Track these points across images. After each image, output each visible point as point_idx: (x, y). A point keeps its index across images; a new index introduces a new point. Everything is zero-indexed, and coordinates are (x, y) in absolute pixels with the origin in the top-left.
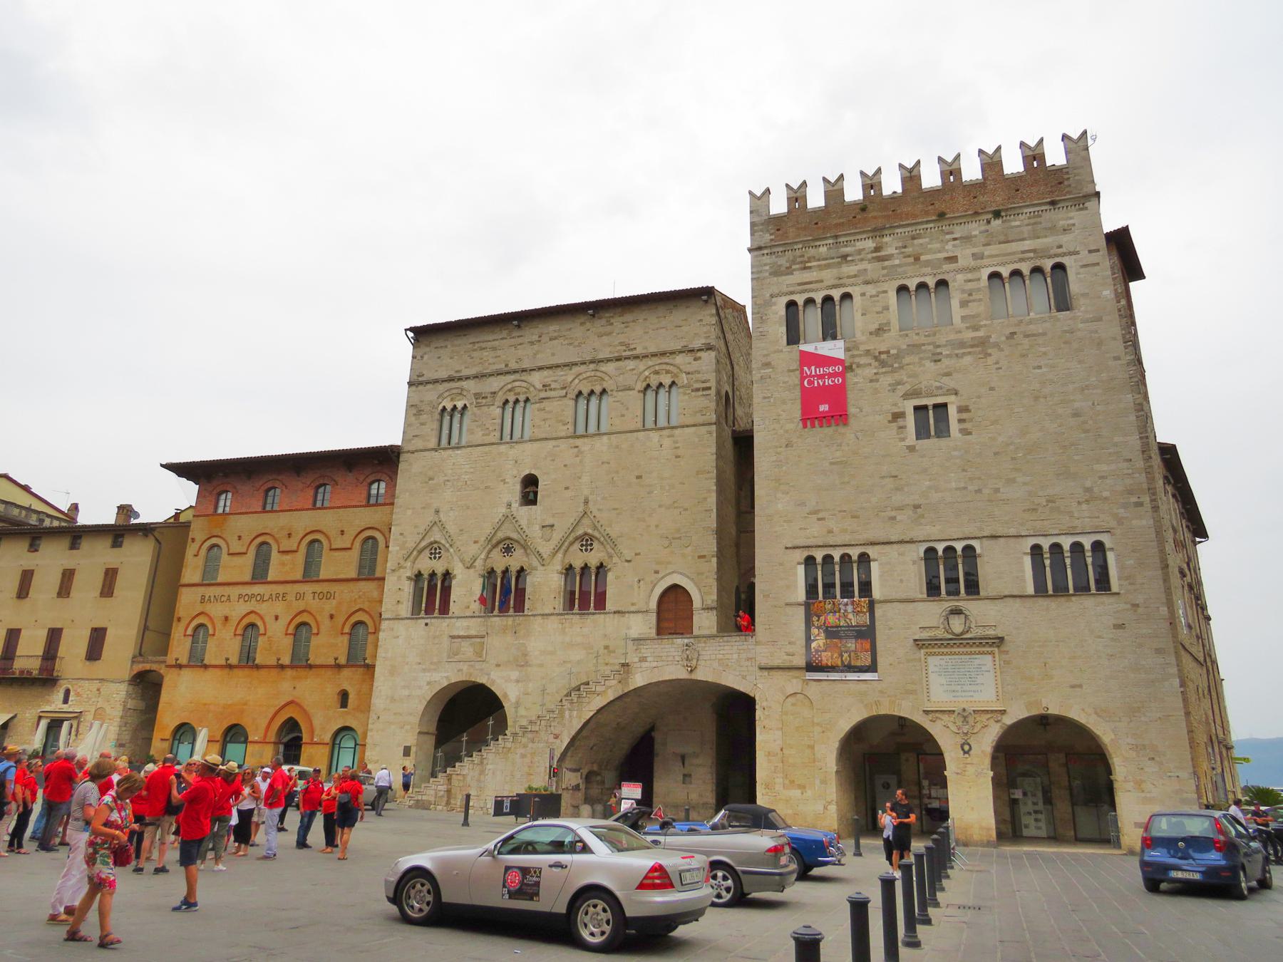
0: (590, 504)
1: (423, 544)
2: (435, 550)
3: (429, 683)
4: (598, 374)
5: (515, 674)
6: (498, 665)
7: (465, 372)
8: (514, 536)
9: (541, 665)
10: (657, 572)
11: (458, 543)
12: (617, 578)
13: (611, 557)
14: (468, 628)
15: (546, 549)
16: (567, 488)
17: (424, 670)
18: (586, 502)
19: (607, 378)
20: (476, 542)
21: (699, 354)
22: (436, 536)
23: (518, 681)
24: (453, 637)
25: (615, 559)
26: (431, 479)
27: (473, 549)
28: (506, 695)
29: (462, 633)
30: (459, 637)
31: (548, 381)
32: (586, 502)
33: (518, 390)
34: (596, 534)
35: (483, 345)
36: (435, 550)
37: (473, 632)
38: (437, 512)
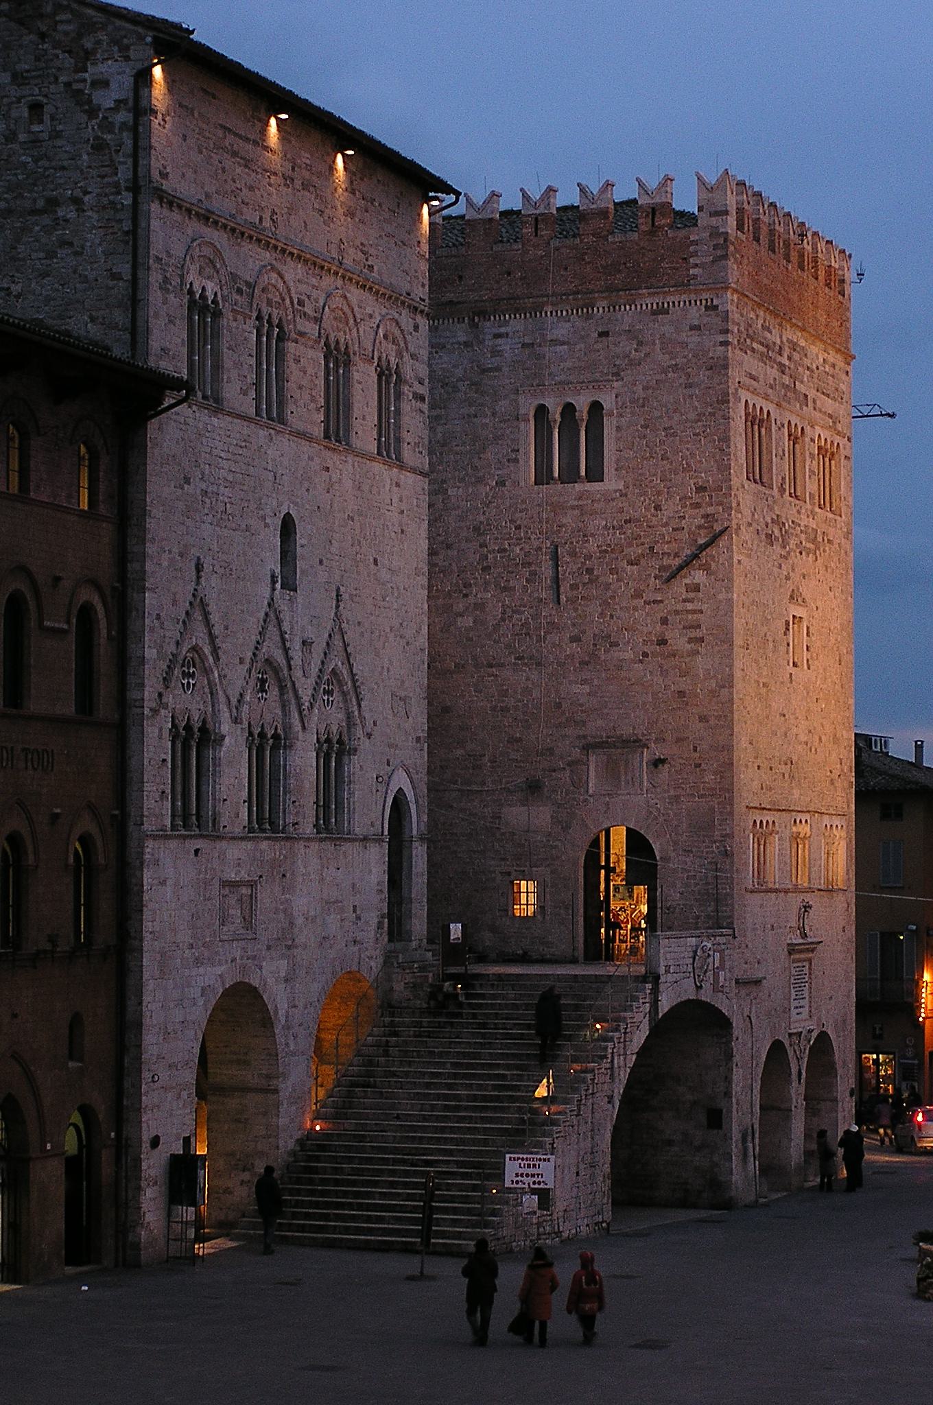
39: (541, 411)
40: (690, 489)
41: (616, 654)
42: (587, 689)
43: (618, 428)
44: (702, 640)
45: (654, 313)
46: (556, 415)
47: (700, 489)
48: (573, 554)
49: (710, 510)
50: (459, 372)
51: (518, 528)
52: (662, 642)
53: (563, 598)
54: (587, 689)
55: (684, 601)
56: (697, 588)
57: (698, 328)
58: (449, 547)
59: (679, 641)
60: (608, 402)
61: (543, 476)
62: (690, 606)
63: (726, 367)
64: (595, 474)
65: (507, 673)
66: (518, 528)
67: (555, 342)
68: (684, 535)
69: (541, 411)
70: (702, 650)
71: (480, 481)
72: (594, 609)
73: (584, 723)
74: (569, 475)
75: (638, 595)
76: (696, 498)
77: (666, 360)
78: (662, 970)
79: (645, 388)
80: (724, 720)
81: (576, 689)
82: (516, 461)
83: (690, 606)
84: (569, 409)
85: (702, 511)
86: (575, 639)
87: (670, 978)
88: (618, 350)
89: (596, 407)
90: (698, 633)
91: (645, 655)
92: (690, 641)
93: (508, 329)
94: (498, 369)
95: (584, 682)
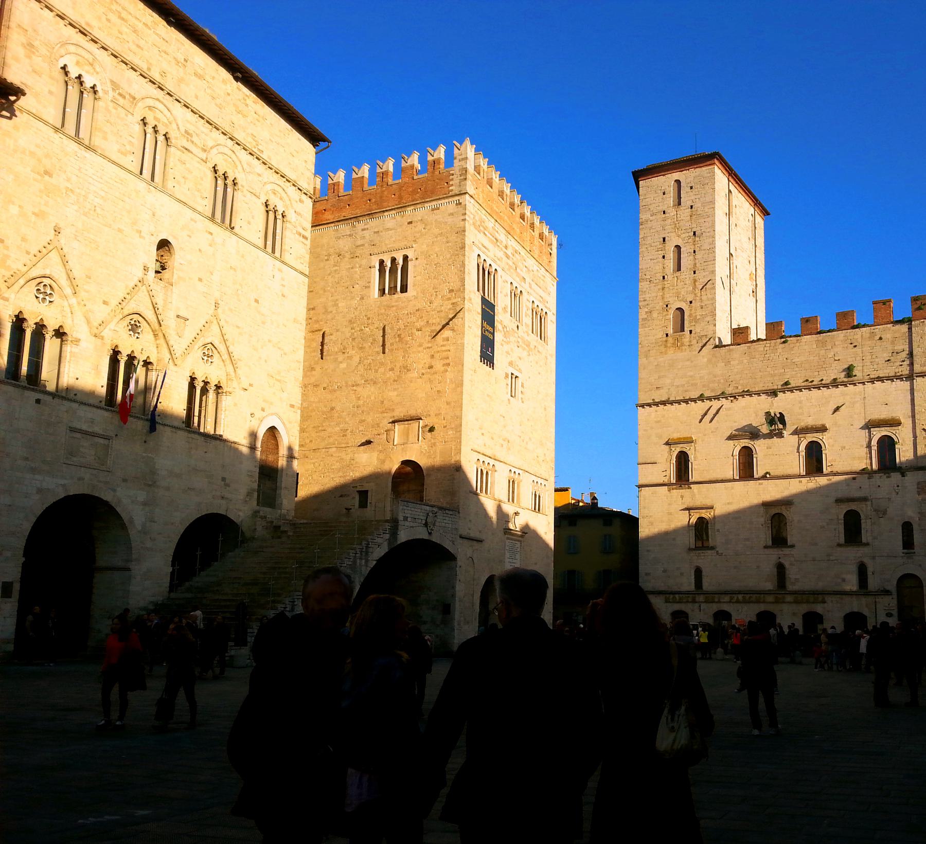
0: (220, 310)
1: (35, 272)
2: (44, 290)
3: (40, 491)
4: (233, 156)
5: (142, 496)
6: (125, 480)
7: (97, 33)
8: (150, 315)
9: (168, 489)
10: (263, 410)
11: (82, 294)
12: (235, 405)
13: (229, 379)
14: (92, 421)
15: (179, 346)
16: (200, 280)
17: (33, 470)
18: (217, 305)
19: (240, 168)
20: (105, 303)
21: (304, 197)
22: (52, 266)
23: (145, 504)
24: (73, 430)
25: (235, 384)
26: (47, 173)
27: (100, 312)
28: (131, 521)
29: (84, 427)
30: (81, 431)
31: (191, 129)
32: (217, 305)
33: (159, 116)
34: (222, 348)
35: (124, 14)
36: (44, 290)
37: (97, 429)
38: (57, 231)
39: (382, 262)
40: (446, 292)
43: (415, 266)
44: (449, 364)
45: (433, 210)
46: (388, 264)
47: (451, 291)
48: (392, 329)
49: (454, 301)
50: (346, 249)
51: (368, 319)
52: (431, 367)
53: (387, 350)
54: (395, 393)
57: (452, 214)
58: (337, 331)
59: (438, 366)
60: (411, 255)
61: (382, 292)
62: (444, 348)
63: (464, 231)
64: (404, 289)
65: (359, 389)
66: (368, 319)
67: (388, 229)
68: (443, 314)
69: (382, 262)
71: (353, 298)
72: (400, 354)
73: (393, 410)
74: (393, 290)
75: (420, 345)
76: (449, 295)
77: (436, 231)
78: (401, 518)
79: (428, 246)
80: (457, 405)
81: (391, 394)
82: (369, 287)
83: (444, 348)
84: (393, 260)
85: (450, 302)
86: (392, 369)
87: (407, 524)
88: (417, 229)
89: (406, 258)
90: (447, 361)
91: (423, 374)
92: (444, 365)
94: (363, 245)
95: (395, 390)
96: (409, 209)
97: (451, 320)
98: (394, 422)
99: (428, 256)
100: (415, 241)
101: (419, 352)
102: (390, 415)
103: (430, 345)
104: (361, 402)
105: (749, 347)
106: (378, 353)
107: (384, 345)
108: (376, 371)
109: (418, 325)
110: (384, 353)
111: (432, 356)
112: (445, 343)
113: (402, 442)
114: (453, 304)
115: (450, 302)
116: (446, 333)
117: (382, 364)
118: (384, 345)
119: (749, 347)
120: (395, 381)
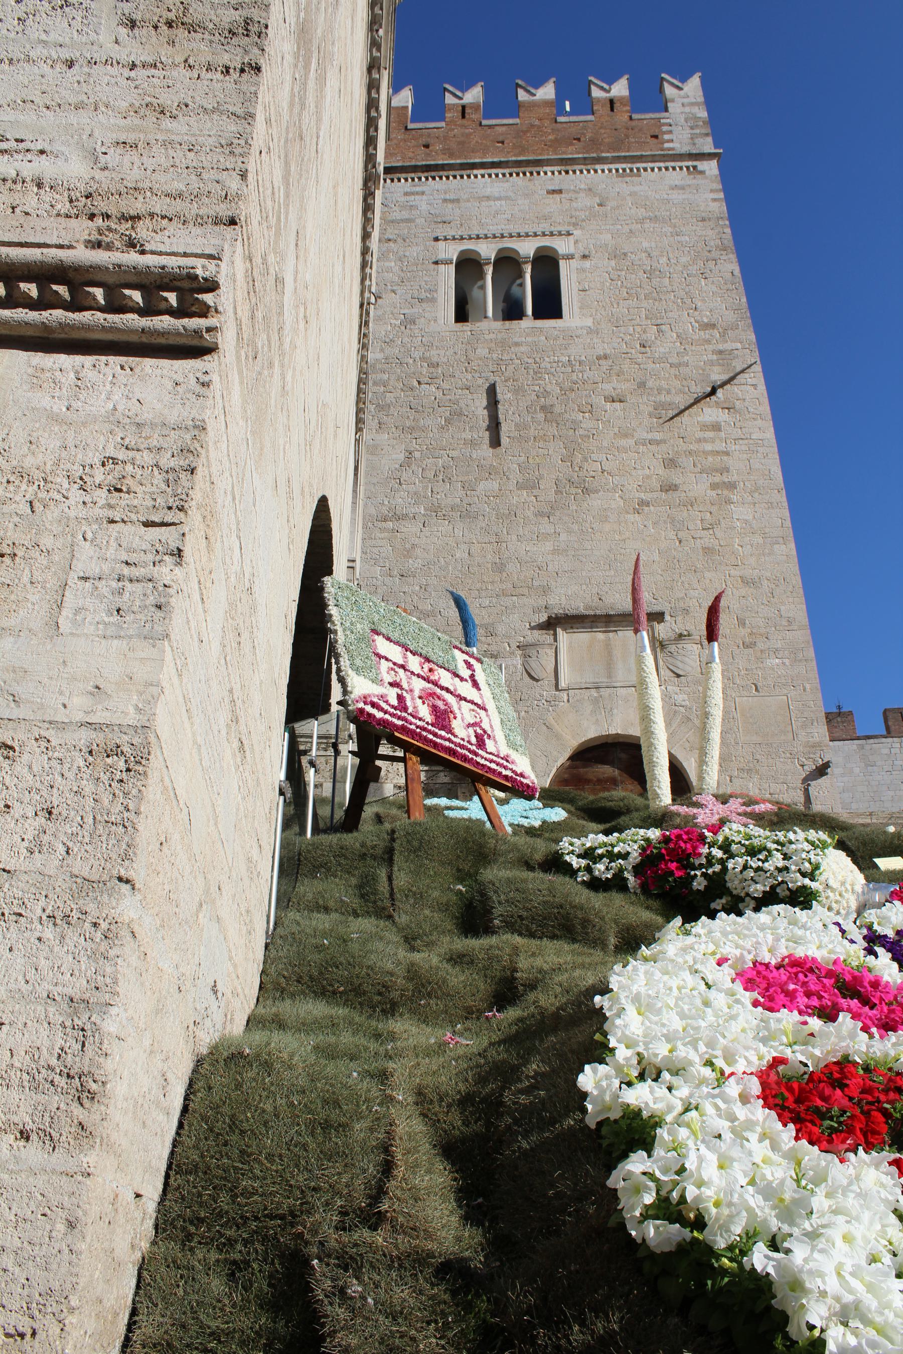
41: (595, 502)
42: (549, 546)
44: (732, 486)
48: (518, 391)
49: (728, 346)
54: (549, 546)
55: (699, 441)
56: (716, 427)
59: (697, 486)
60: (562, 246)
65: (410, 529)
70: (734, 498)
73: (546, 590)
82: (433, 300)
86: (530, 485)
91: (643, 503)
92: (714, 486)
93: (424, 188)
95: (540, 537)
96: (548, 169)
97: (722, 385)
98: (552, 624)
99: (618, 255)
100: (575, 225)
101: (625, 450)
102: (531, 601)
103: (658, 436)
104: (413, 564)
105: (862, 747)
106: (472, 443)
107: (494, 426)
108: (468, 487)
109: (608, 388)
110: (495, 442)
111: (670, 463)
112: (710, 434)
113: (589, 678)
114: (721, 352)
115: (710, 347)
116: (709, 413)
117: (491, 472)
118: (494, 426)
119: (862, 747)
120: (540, 514)
